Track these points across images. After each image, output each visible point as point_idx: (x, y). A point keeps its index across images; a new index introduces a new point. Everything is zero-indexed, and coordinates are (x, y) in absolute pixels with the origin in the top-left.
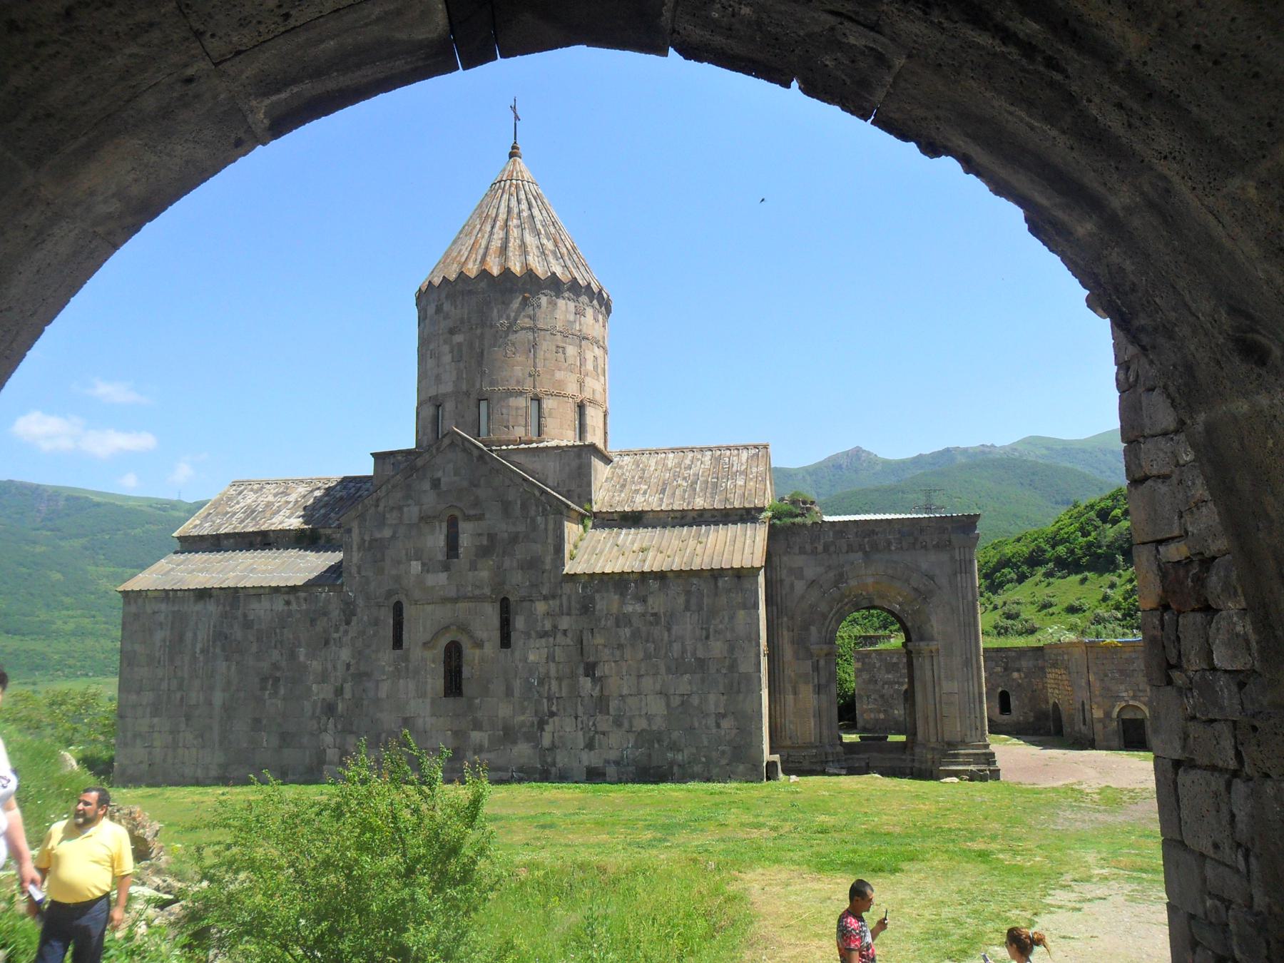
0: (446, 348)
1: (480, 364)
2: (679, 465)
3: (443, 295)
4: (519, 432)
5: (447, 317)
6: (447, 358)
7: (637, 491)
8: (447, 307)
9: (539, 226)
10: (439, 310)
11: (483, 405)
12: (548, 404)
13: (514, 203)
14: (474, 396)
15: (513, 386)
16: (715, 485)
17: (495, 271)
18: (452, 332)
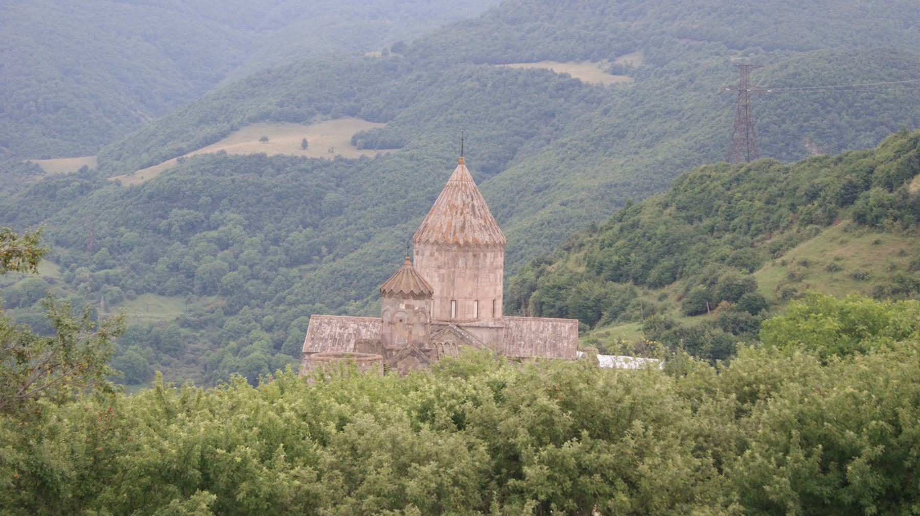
0: (436, 275)
1: (453, 285)
2: (538, 328)
3: (435, 248)
4: (469, 316)
5: (436, 259)
6: (437, 279)
7: (520, 345)
8: (436, 254)
9: (477, 212)
10: (432, 255)
11: (453, 303)
12: (482, 303)
13: (464, 197)
14: (450, 299)
15: (467, 295)
16: (555, 345)
17: (461, 242)
18: (439, 267)
